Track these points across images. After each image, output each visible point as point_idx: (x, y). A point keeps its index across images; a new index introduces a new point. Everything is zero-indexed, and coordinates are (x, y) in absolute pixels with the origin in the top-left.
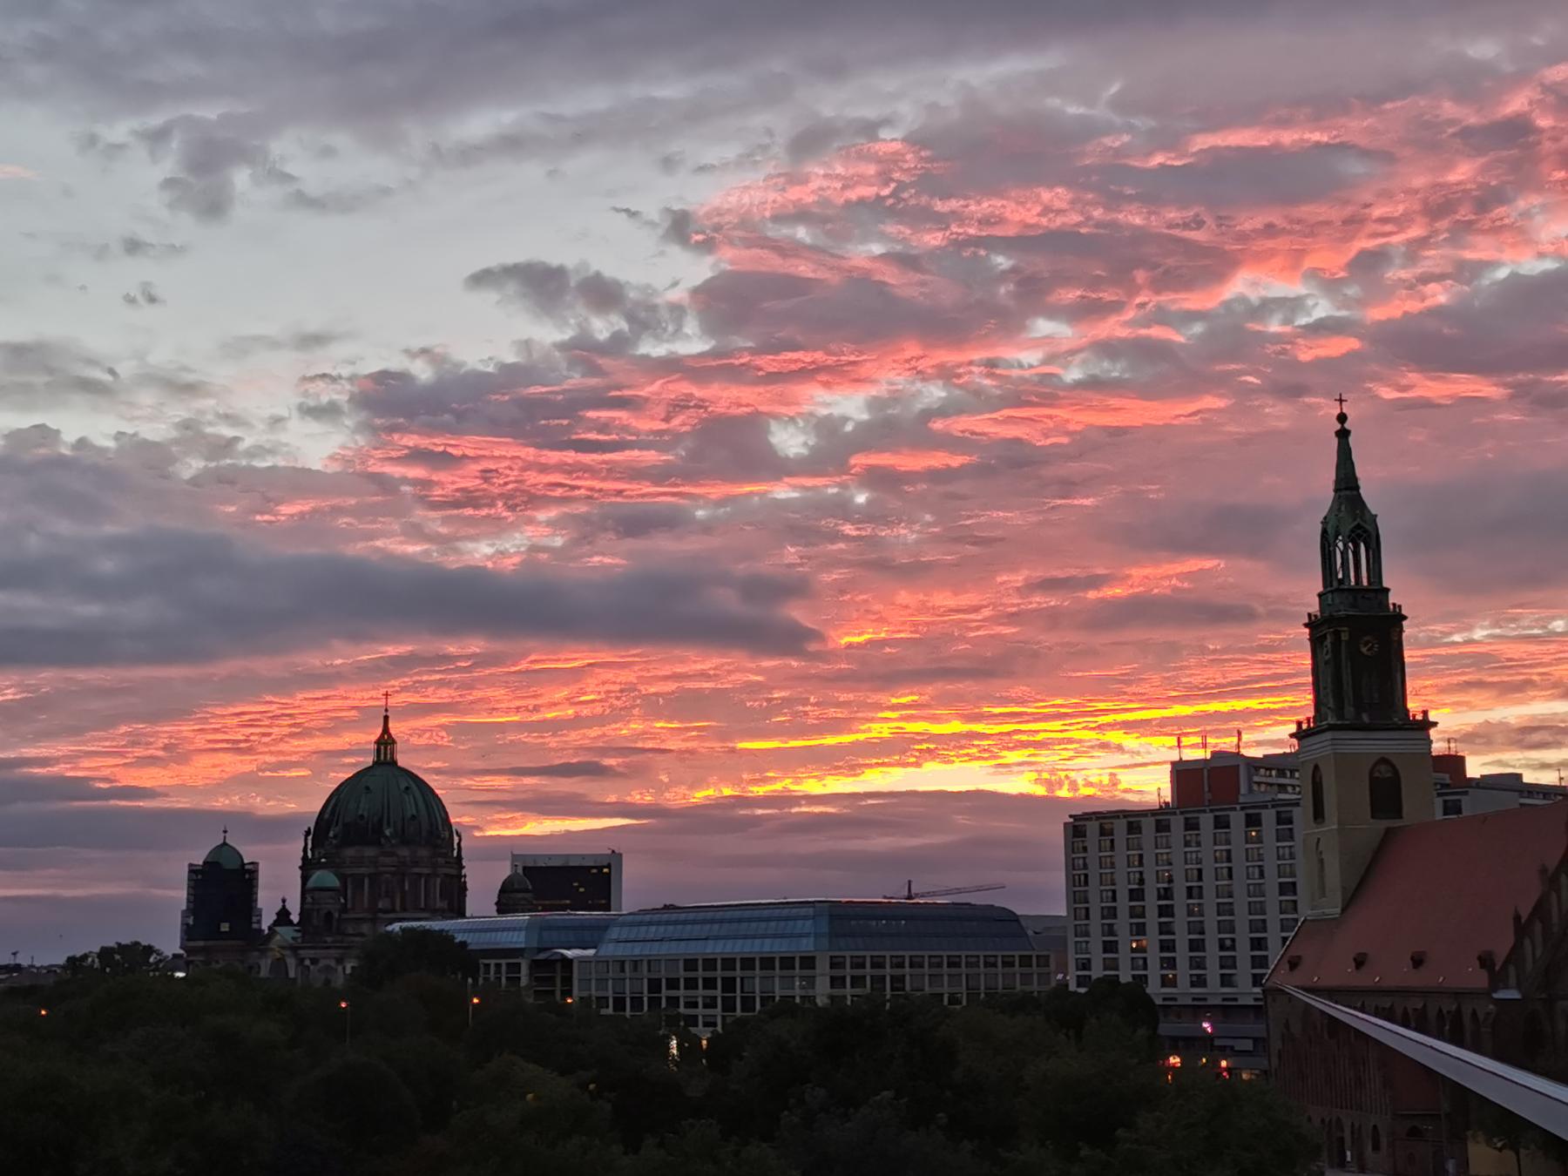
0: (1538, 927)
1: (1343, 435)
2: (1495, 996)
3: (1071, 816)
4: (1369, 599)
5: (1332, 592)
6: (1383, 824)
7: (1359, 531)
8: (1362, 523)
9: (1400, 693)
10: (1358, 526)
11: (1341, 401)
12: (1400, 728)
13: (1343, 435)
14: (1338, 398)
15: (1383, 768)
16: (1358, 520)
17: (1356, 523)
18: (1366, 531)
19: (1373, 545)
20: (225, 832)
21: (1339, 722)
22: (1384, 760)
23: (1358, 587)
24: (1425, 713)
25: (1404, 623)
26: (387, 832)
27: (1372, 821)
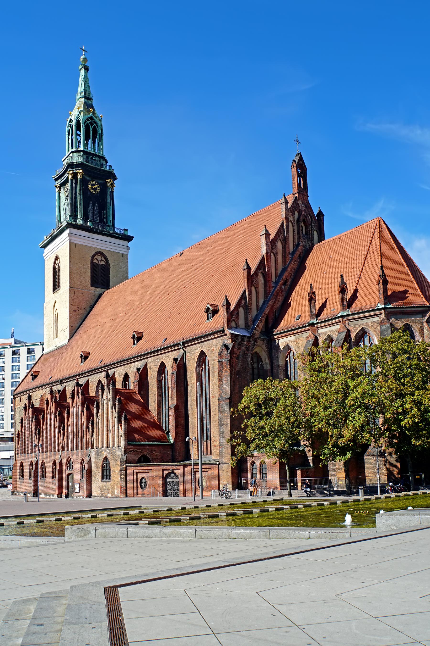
0: (261, 280)
4: (95, 160)
5: (73, 152)
6: (99, 291)
7: (92, 121)
8: (93, 117)
9: (110, 218)
10: (91, 118)
15: (99, 258)
17: (90, 115)
18: (95, 122)
19: (99, 131)
22: (100, 253)
25: (115, 181)
27: (92, 288)
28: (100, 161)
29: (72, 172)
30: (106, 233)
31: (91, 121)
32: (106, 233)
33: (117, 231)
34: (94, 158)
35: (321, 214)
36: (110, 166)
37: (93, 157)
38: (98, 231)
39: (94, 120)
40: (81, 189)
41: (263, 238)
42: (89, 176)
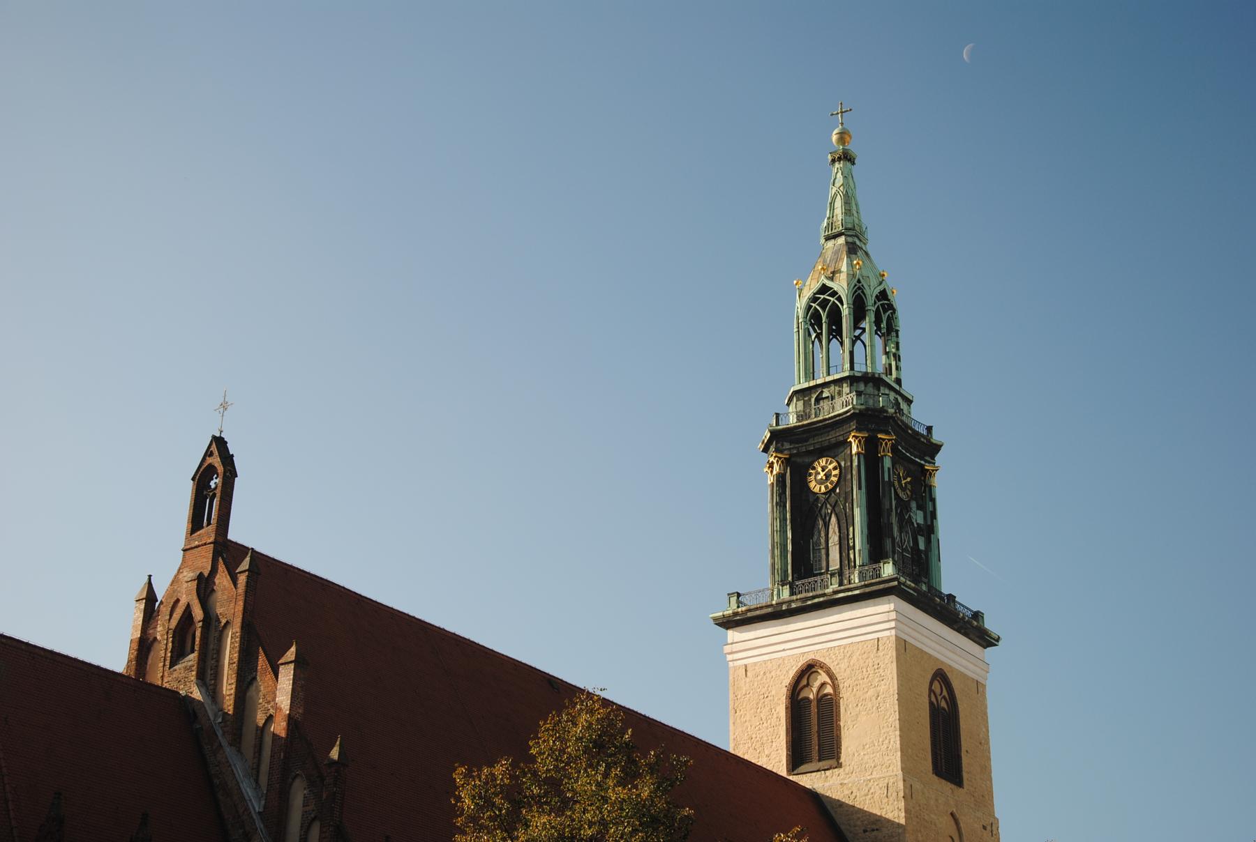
4: (828, 397)
8: (829, 284)
10: (824, 289)
12: (832, 603)
18: (834, 294)
23: (806, 385)
28: (840, 393)
30: (816, 600)
31: (822, 297)
32: (816, 600)
34: (824, 396)
37: (822, 392)
38: (794, 605)
39: (832, 288)
40: (777, 503)
42: (809, 453)
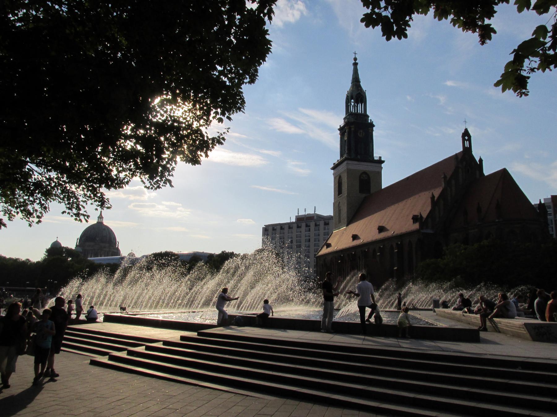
1: (355, 64)
2: (422, 231)
3: (265, 225)
10: (359, 93)
11: (355, 54)
13: (355, 64)
14: (354, 52)
15: (364, 176)
16: (359, 91)
17: (358, 92)
20: (57, 238)
21: (349, 157)
22: (365, 173)
24: (380, 157)
26: (97, 239)
29: (348, 127)
33: (375, 159)
35: (481, 160)
36: (371, 120)
41: (443, 179)
